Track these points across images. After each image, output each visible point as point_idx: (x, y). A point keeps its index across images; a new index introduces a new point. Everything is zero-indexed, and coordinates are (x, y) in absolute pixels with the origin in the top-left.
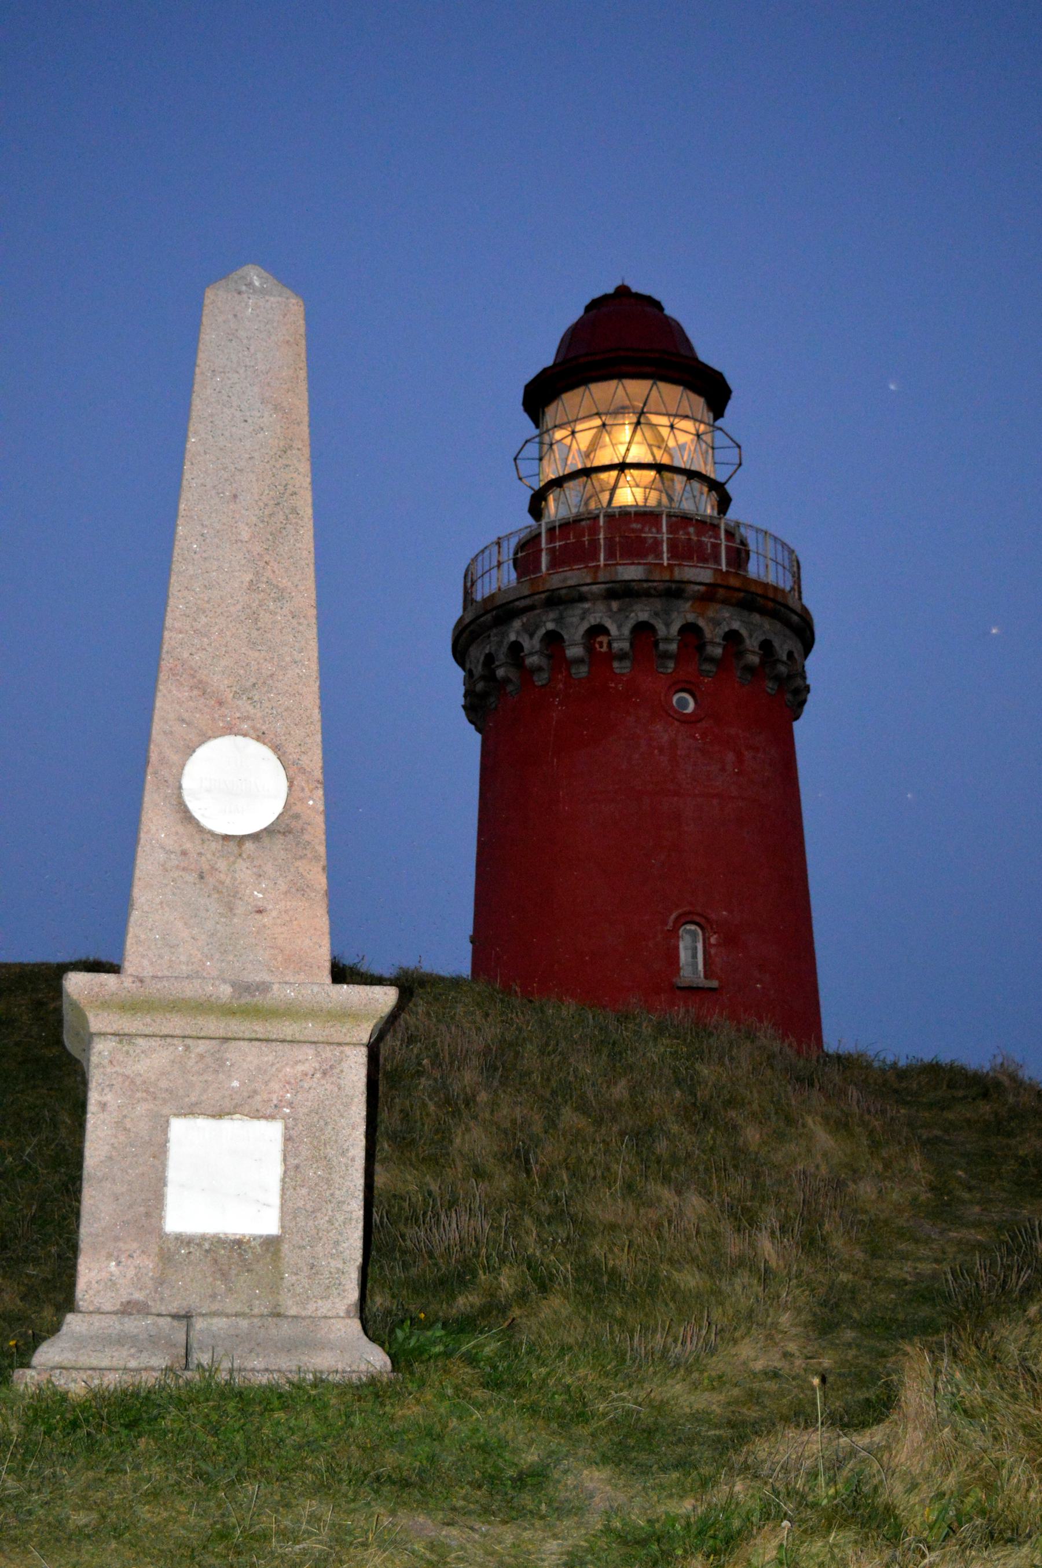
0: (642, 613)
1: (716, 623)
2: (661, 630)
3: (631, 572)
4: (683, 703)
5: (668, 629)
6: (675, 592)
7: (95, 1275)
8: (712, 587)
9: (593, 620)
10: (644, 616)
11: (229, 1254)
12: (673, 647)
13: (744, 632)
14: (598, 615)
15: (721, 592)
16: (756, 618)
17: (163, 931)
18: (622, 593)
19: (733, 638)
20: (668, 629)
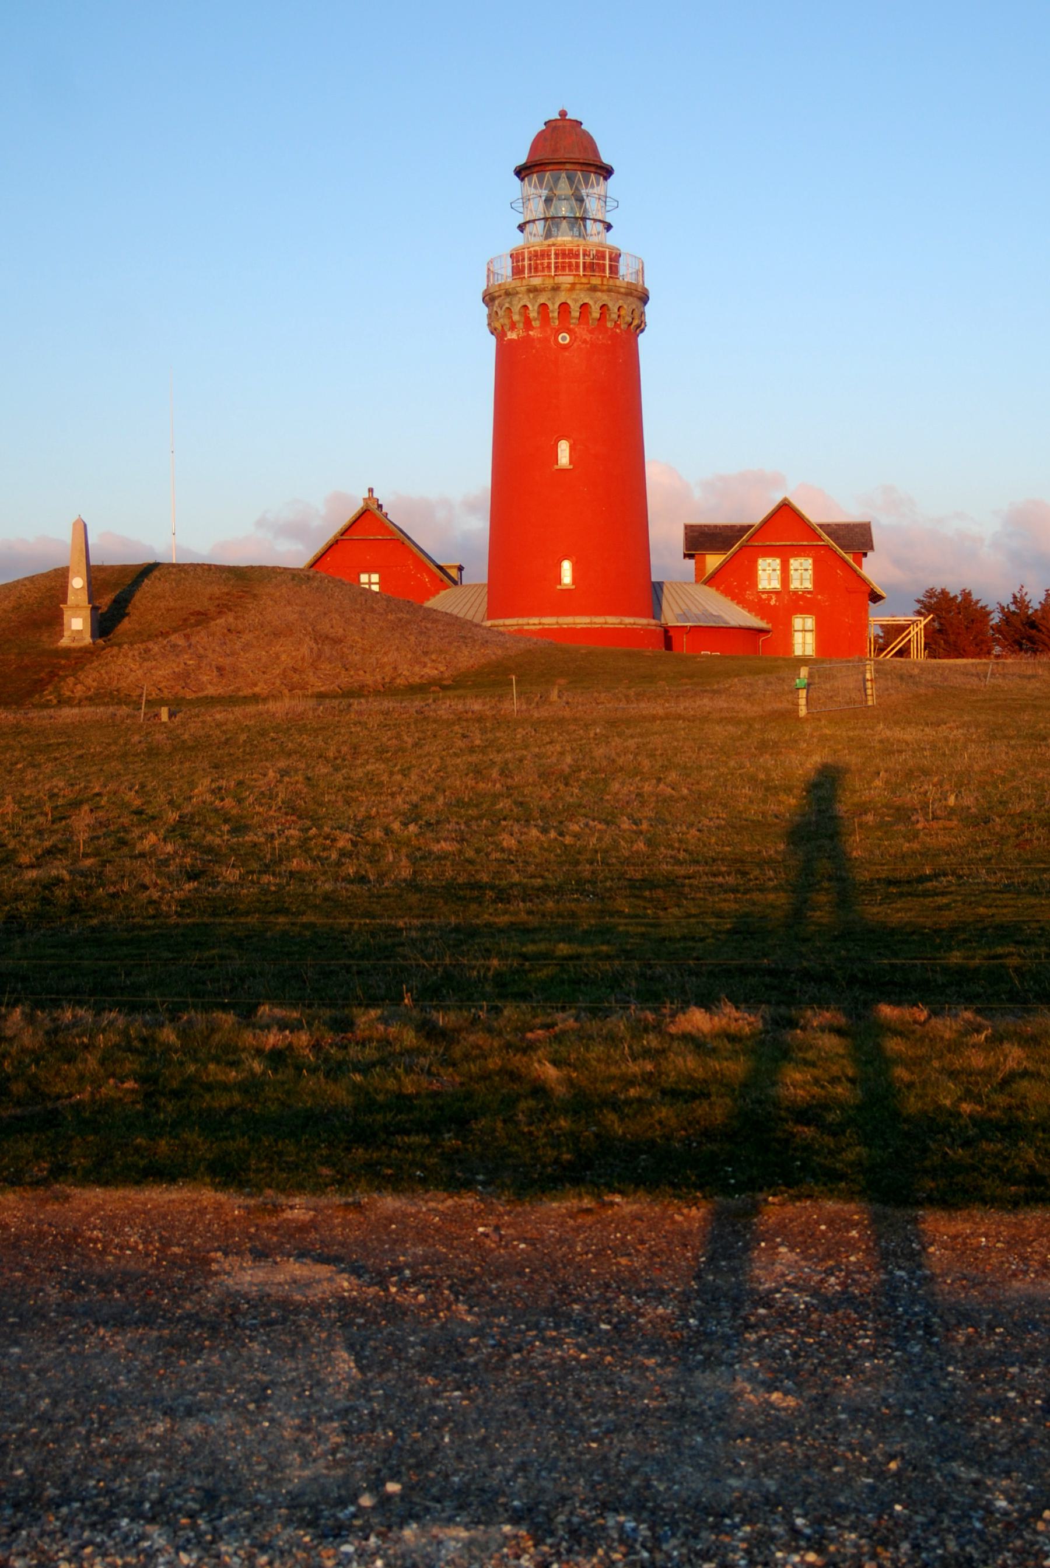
0: (542, 300)
1: (576, 300)
2: (551, 307)
3: (536, 281)
4: (564, 338)
5: (554, 308)
6: (556, 289)
7: (66, 633)
8: (574, 284)
9: (522, 303)
10: (542, 301)
11: (79, 631)
12: (556, 314)
13: (591, 303)
14: (525, 301)
15: (578, 287)
16: (599, 294)
17: (71, 598)
18: (534, 290)
19: (585, 306)
20: (554, 308)
